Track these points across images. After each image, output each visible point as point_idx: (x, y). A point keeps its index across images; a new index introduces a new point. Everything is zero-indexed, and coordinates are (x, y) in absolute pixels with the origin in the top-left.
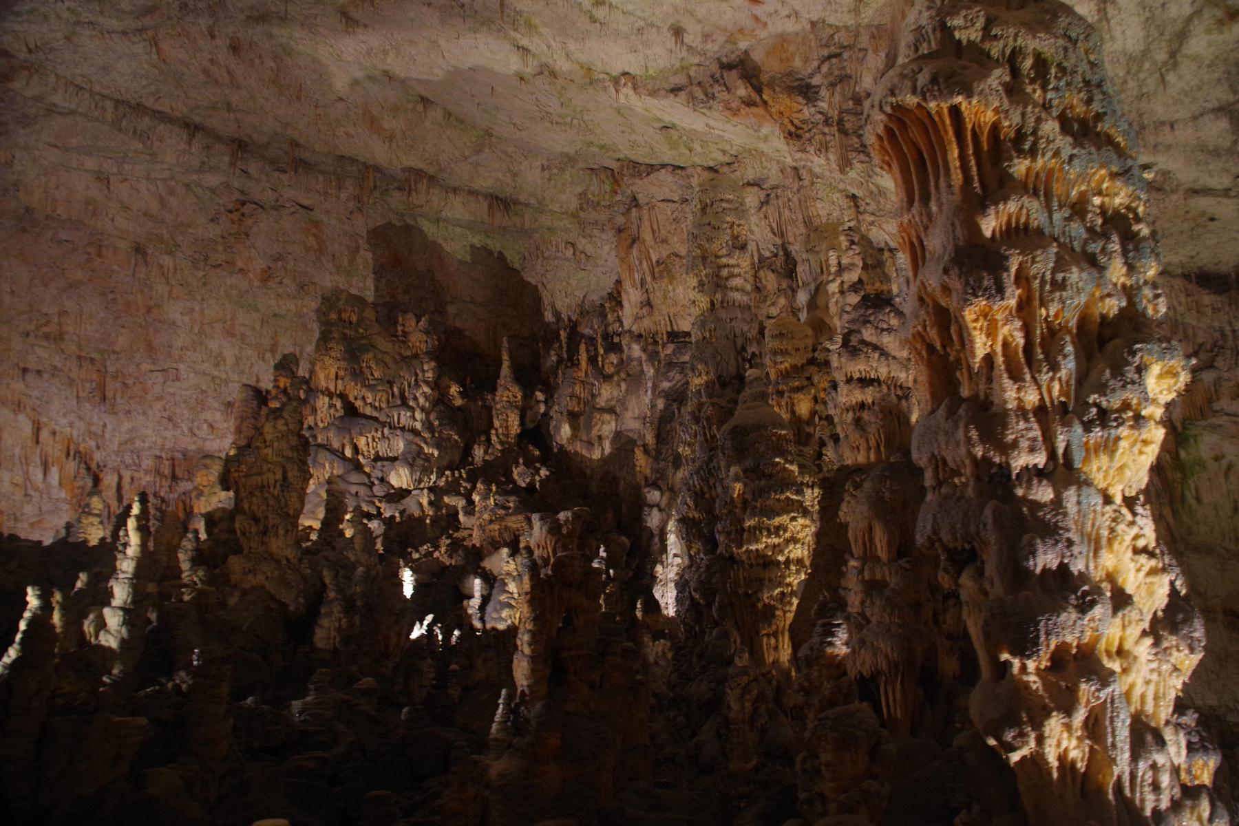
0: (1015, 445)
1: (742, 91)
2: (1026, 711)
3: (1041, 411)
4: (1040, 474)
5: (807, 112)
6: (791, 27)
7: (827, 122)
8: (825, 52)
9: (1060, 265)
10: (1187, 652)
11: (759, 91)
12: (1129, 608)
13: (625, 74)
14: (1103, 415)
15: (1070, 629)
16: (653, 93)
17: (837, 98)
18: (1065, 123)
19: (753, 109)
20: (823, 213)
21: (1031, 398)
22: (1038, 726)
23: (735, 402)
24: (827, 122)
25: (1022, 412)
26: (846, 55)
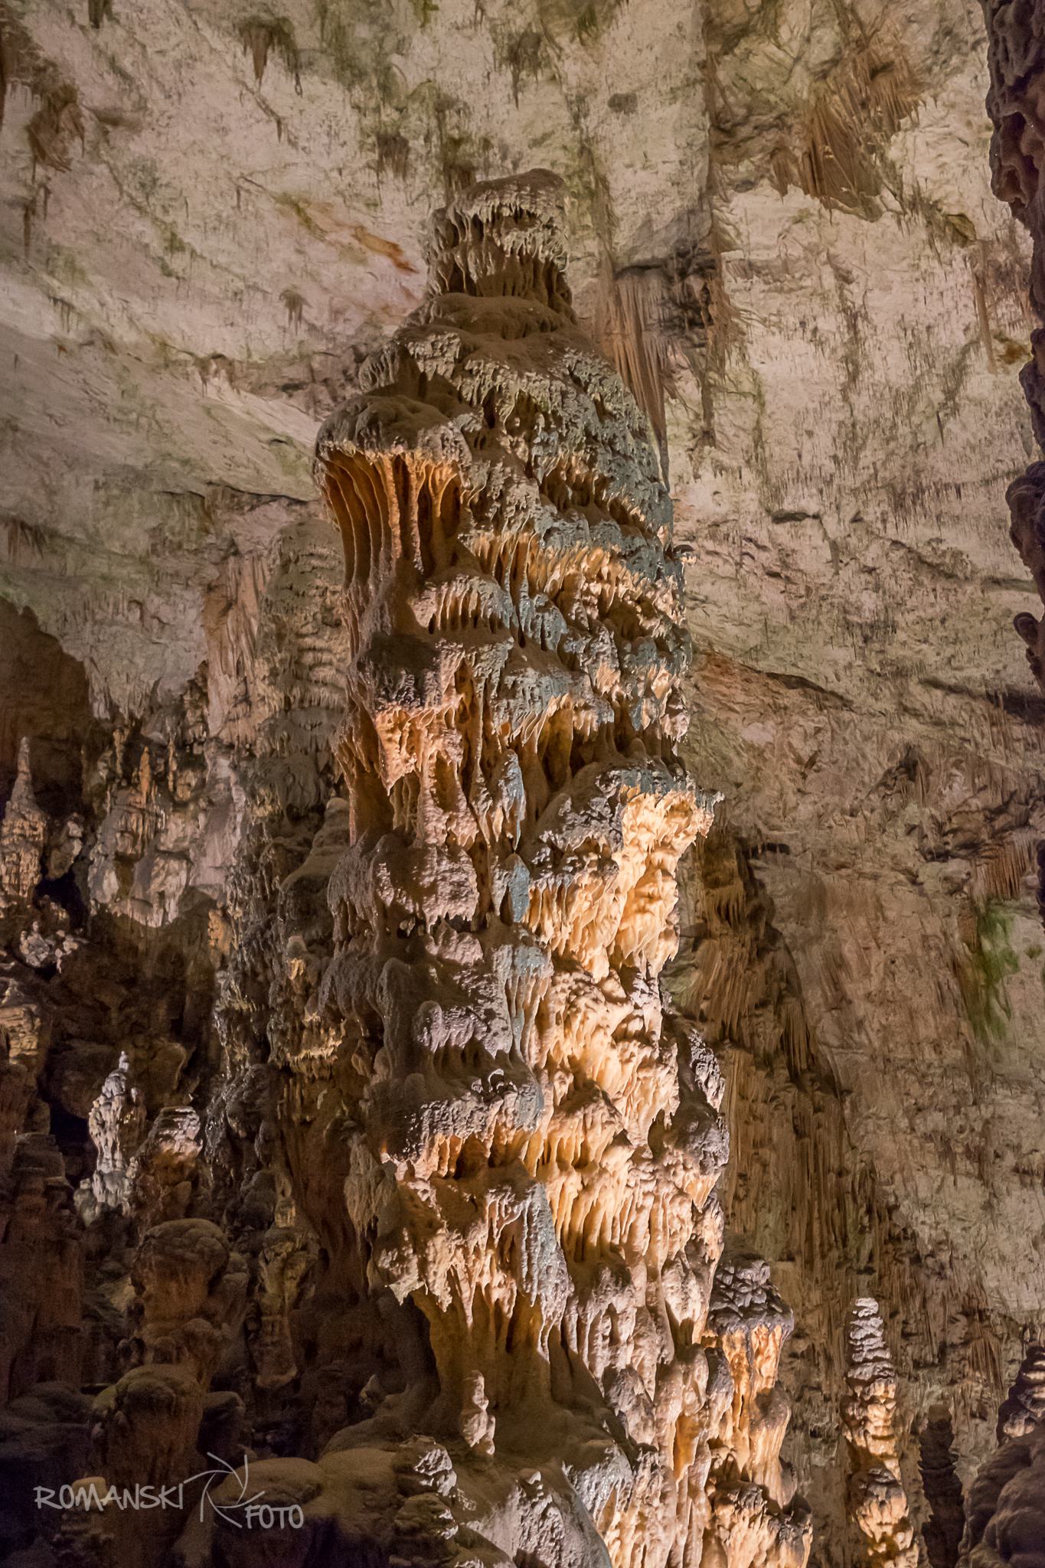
0: (433, 889)
2: (408, 1227)
3: (477, 850)
4: (461, 926)
9: (512, 665)
10: (697, 1170)
12: (592, 1106)
13: (217, 357)
14: (558, 855)
15: (462, 1121)
16: (257, 389)
18: (551, 489)
21: (466, 831)
22: (420, 1248)
23: (308, 843)
25: (451, 850)
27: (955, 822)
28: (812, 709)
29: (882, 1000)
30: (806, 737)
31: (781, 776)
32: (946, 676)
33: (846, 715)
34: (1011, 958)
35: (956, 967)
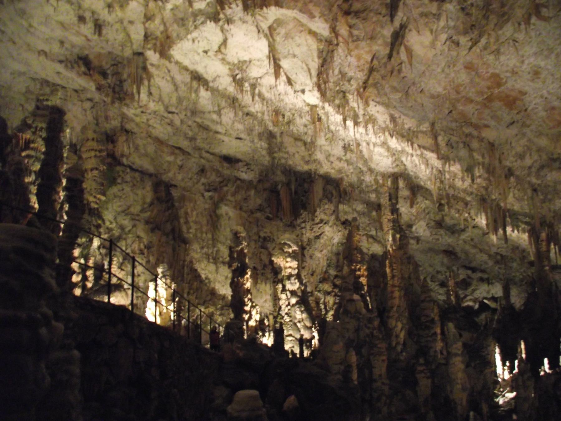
1: (83, 69)
5: (104, 82)
6: (103, 51)
7: (109, 87)
8: (113, 63)
11: (89, 70)
13: (42, 51)
16: (53, 60)
17: (114, 80)
19: (86, 77)
20: (111, 115)
24: (109, 87)
26: (119, 65)
27: (212, 184)
28: (181, 155)
29: (196, 222)
30: (181, 161)
31: (174, 169)
32: (211, 151)
33: (189, 157)
34: (222, 215)
35: (211, 216)
